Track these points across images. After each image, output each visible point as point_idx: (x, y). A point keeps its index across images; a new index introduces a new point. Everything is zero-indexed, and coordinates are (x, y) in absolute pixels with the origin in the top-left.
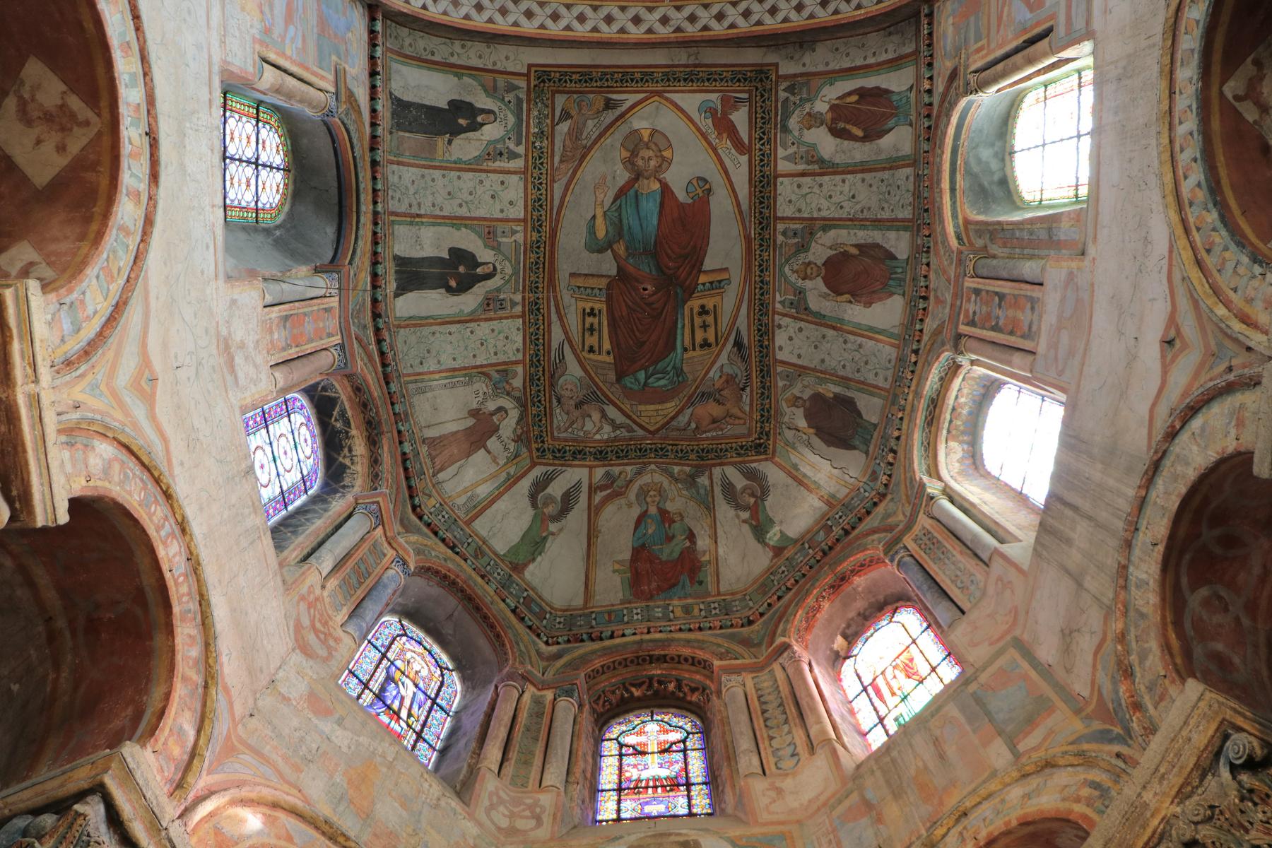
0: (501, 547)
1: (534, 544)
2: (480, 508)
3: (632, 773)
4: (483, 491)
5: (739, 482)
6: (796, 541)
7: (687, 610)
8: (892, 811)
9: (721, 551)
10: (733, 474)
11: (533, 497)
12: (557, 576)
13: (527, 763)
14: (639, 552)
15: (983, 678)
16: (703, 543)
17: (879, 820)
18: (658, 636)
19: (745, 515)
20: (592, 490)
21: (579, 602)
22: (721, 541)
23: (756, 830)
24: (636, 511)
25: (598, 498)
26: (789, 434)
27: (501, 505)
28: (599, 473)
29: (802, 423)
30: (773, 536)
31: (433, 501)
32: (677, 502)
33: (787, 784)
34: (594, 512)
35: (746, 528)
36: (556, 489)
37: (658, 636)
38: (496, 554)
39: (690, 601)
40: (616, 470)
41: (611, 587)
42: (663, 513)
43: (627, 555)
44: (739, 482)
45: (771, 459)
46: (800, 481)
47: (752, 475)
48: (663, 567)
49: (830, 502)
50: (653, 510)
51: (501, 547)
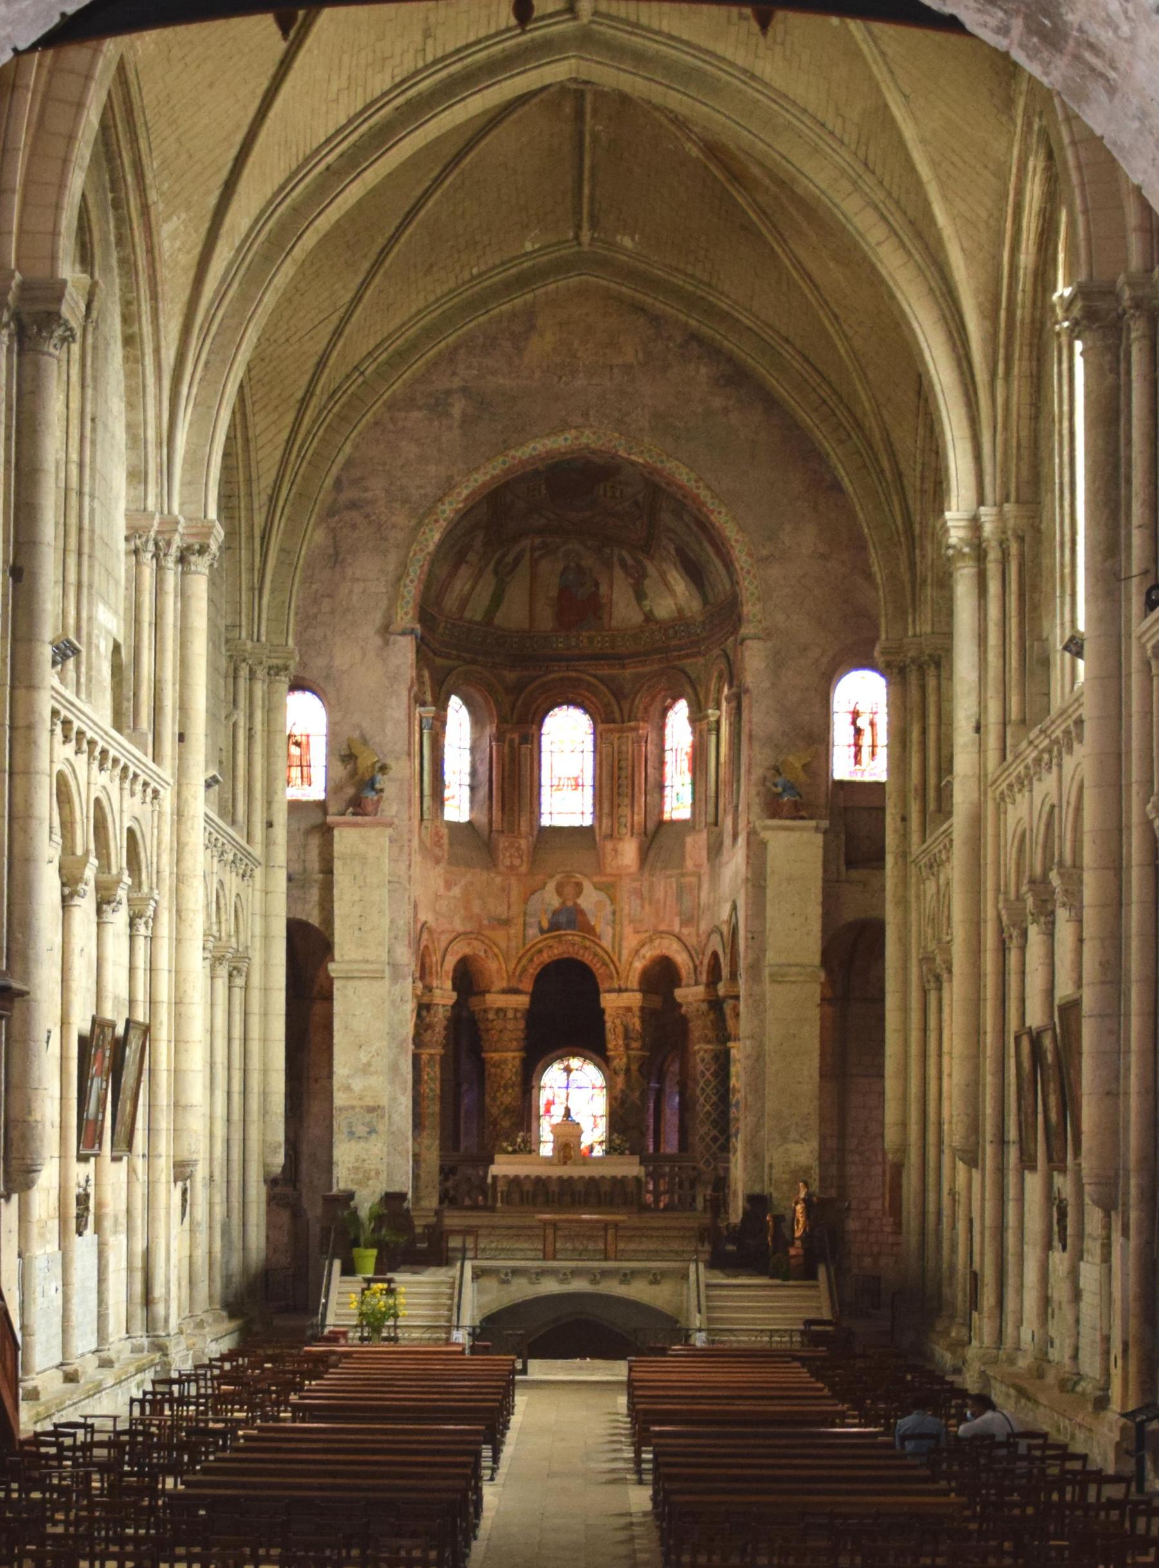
0: (478, 618)
1: (497, 599)
2: (464, 602)
3: (557, 772)
4: (465, 592)
5: (630, 562)
6: (657, 622)
7: (591, 639)
8: (647, 906)
9: (615, 596)
10: (624, 553)
11: (496, 572)
12: (514, 613)
13: (512, 809)
14: (564, 591)
15: (687, 879)
16: (603, 589)
17: (643, 907)
18: (574, 674)
19: (631, 581)
20: (533, 549)
21: (526, 626)
22: (615, 588)
23: (604, 879)
24: (560, 567)
25: (537, 554)
26: (664, 553)
27: (478, 588)
28: (538, 541)
29: (673, 552)
30: (646, 603)
31: (443, 624)
32: (588, 562)
33: (620, 846)
34: (534, 563)
35: (630, 590)
36: (509, 559)
37: (574, 674)
38: (478, 623)
39: (592, 633)
40: (549, 540)
41: (546, 620)
42: (579, 566)
43: (554, 593)
44: (630, 562)
45: (652, 558)
46: (666, 584)
47: (638, 562)
48: (579, 606)
49: (680, 610)
50: (572, 564)
51: (478, 618)
